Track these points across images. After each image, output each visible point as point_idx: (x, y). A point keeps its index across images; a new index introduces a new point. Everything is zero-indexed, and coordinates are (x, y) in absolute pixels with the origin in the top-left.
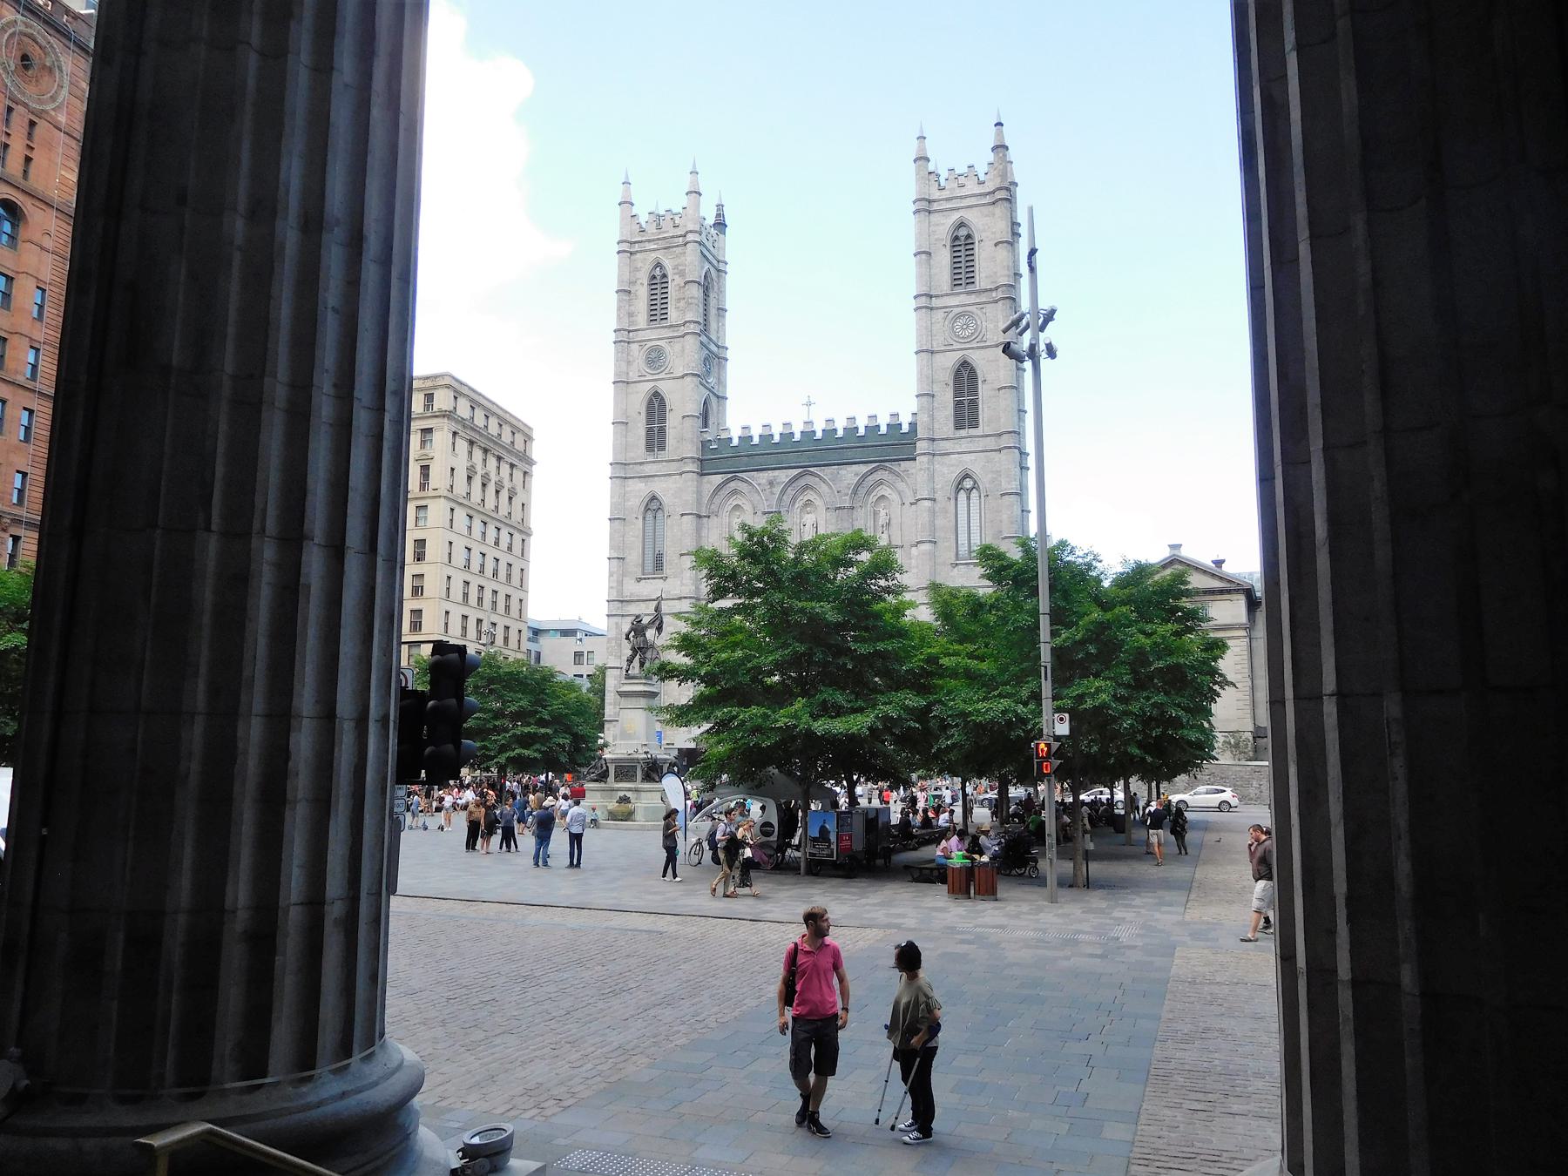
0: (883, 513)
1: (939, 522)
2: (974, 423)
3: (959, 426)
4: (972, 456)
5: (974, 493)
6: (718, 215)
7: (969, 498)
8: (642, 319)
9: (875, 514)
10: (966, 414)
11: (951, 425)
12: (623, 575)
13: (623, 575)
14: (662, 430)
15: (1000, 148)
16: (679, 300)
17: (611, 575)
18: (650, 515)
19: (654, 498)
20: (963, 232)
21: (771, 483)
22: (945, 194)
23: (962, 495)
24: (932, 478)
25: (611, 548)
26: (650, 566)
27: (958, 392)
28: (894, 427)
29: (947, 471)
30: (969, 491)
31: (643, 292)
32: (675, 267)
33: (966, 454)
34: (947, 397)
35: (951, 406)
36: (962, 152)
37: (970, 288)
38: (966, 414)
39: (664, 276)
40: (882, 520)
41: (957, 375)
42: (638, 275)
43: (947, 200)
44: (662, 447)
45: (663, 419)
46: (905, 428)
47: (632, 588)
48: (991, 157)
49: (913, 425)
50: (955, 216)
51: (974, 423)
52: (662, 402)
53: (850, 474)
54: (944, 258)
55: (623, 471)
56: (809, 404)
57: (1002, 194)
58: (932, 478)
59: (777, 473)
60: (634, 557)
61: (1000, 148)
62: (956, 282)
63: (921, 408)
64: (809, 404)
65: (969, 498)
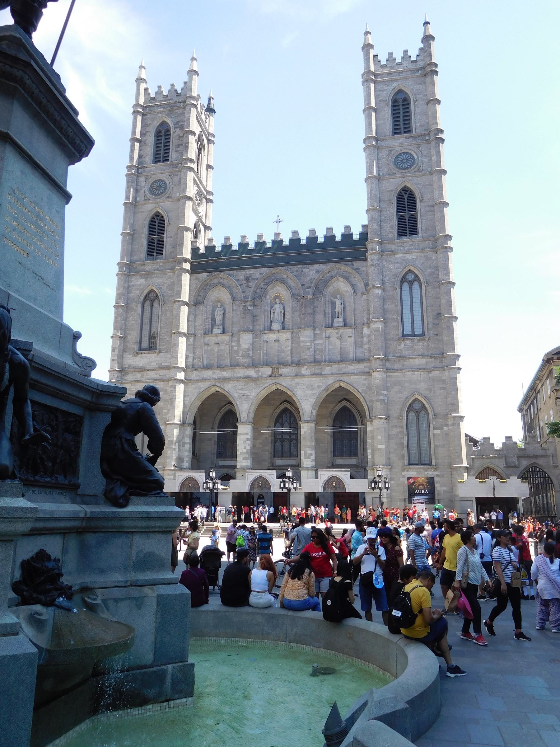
0: (338, 303)
1: (389, 306)
2: (414, 231)
3: (401, 234)
4: (414, 256)
5: (416, 285)
6: (209, 104)
7: (411, 289)
8: (149, 158)
9: (333, 304)
10: (407, 226)
11: (396, 233)
12: (124, 350)
13: (124, 350)
14: (161, 241)
15: (428, 39)
16: (178, 146)
17: (113, 350)
18: (148, 304)
19: (152, 290)
20: (400, 97)
21: (247, 279)
22: (387, 70)
23: (406, 286)
24: (382, 272)
25: (115, 328)
26: (145, 344)
27: (400, 208)
28: (347, 236)
29: (394, 267)
30: (411, 283)
31: (151, 140)
32: (176, 123)
33: (409, 254)
34: (392, 212)
35: (395, 218)
36: (398, 42)
37: (408, 135)
38: (407, 226)
39: (168, 130)
40: (338, 308)
41: (400, 199)
42: (148, 129)
43: (389, 74)
44: (160, 252)
45: (162, 231)
46: (356, 237)
47: (131, 360)
48: (422, 46)
49: (364, 236)
50: (395, 84)
51: (414, 231)
52: (162, 220)
53: (312, 272)
54: (388, 112)
55: (128, 270)
56: (278, 222)
57: (428, 69)
58: (382, 272)
59: (252, 271)
60: (133, 336)
61: (428, 39)
62: (396, 131)
63: (371, 220)
64: (278, 222)
65: (411, 289)
